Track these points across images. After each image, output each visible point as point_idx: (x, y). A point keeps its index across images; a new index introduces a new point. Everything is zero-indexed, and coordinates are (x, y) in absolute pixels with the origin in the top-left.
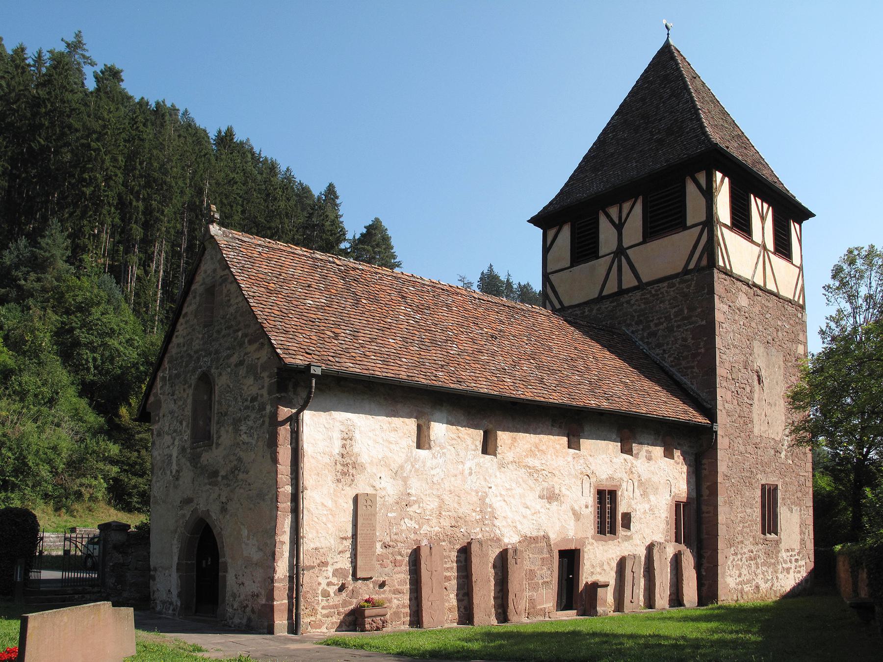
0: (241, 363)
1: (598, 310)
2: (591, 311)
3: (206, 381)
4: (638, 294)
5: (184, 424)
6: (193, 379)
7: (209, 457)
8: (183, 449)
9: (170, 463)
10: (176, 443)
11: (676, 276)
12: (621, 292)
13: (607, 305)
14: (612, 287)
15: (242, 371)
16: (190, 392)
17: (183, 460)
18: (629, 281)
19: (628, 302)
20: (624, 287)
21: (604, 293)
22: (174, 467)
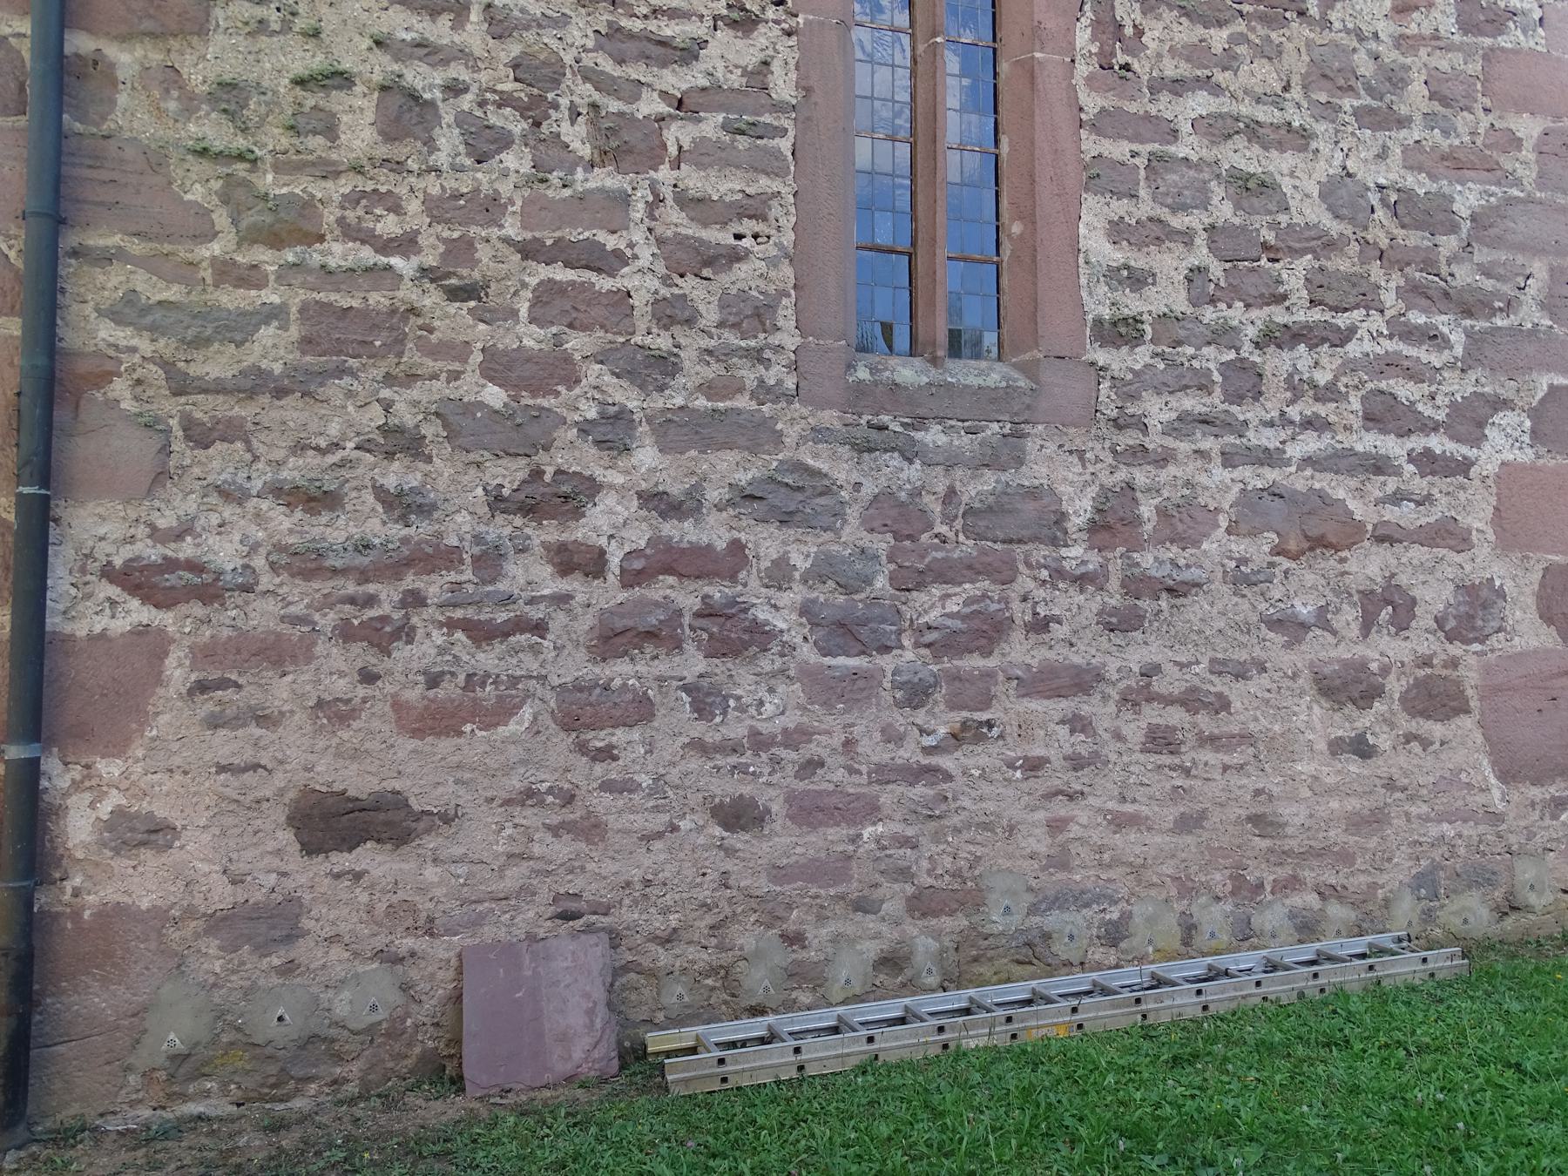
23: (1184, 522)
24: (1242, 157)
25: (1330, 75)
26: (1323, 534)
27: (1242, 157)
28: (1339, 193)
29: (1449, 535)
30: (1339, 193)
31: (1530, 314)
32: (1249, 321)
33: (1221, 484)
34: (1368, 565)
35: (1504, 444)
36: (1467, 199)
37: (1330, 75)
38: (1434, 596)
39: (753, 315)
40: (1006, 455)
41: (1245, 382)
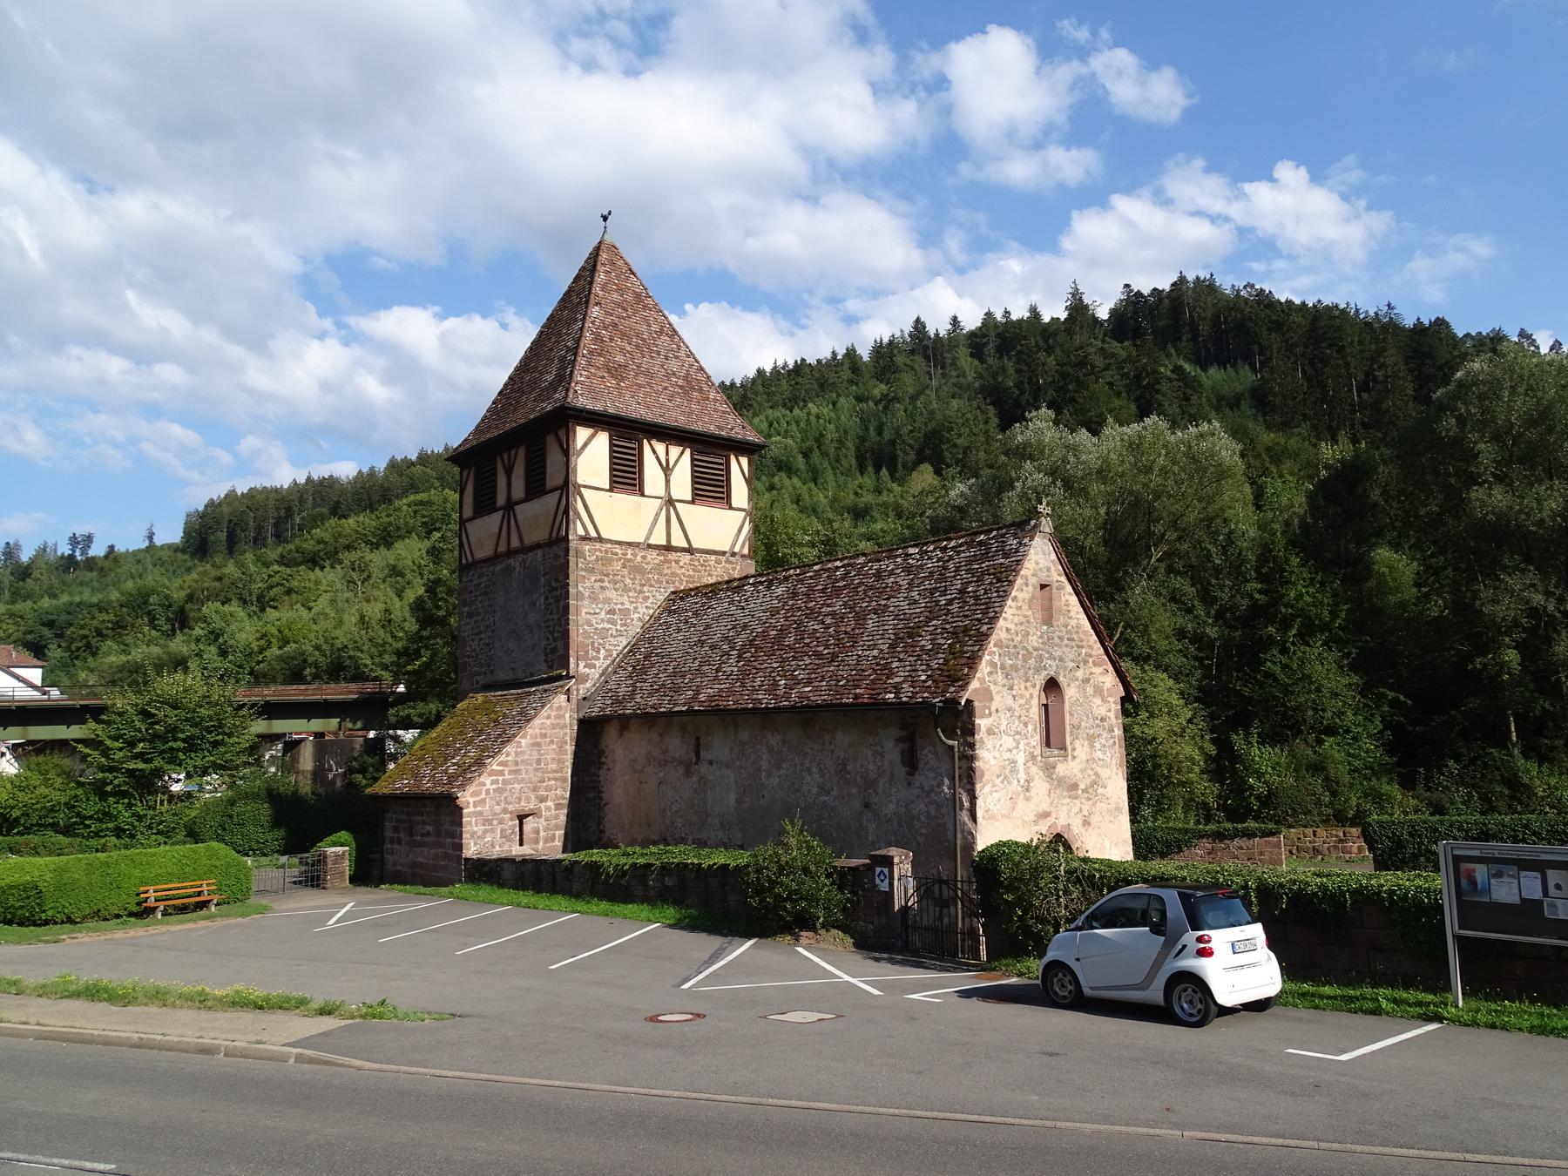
0: (1086, 681)
1: (644, 557)
2: (635, 555)
3: (1052, 686)
4: (688, 557)
5: (1030, 727)
6: (1040, 680)
7: (1062, 769)
8: (1033, 757)
9: (1014, 770)
10: (1021, 746)
11: (724, 553)
12: (668, 548)
13: (653, 556)
14: (659, 538)
15: (1090, 690)
16: (1036, 693)
17: (1034, 769)
18: (678, 540)
19: (677, 562)
20: (674, 543)
21: (651, 541)
22: (1022, 776)
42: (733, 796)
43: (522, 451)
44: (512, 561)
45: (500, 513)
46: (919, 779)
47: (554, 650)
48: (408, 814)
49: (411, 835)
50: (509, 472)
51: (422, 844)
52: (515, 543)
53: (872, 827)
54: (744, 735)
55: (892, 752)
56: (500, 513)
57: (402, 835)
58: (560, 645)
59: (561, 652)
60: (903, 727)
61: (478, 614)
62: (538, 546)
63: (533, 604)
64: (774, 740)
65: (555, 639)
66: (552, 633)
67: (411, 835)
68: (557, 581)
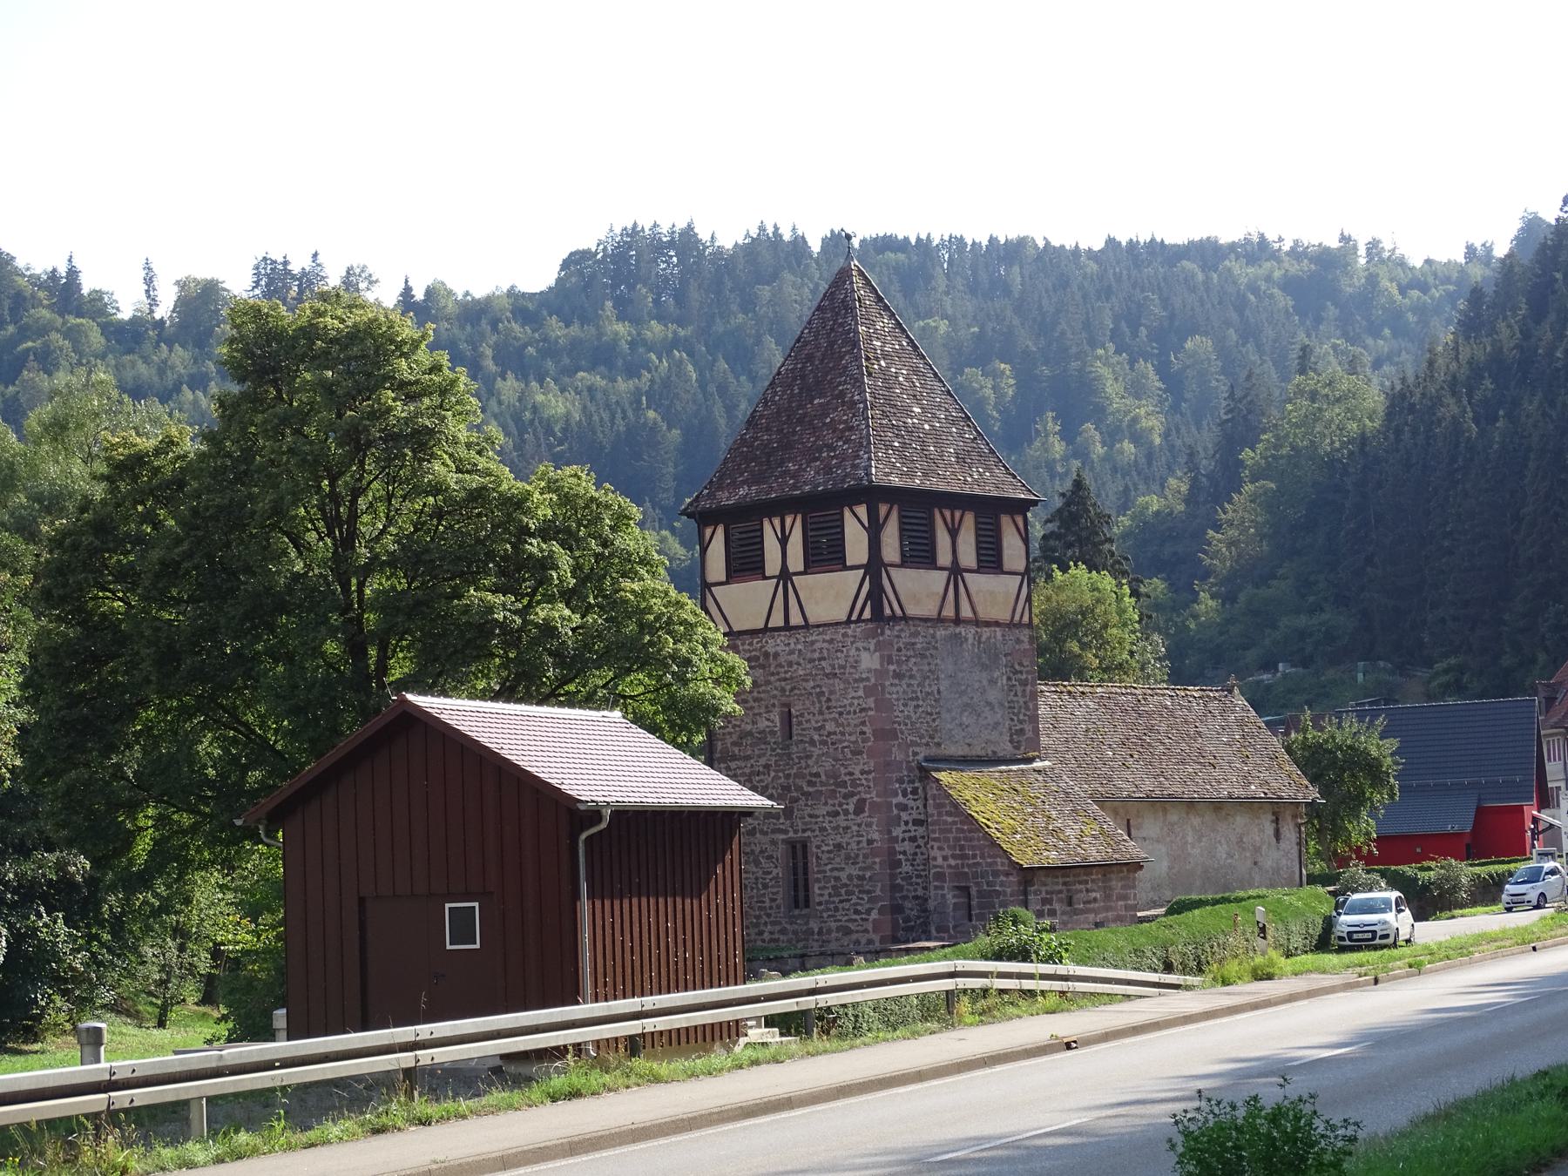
23: (829, 931)
24: (836, 874)
25: (848, 857)
26: (847, 932)
27: (836, 874)
28: (850, 877)
29: (866, 931)
30: (850, 877)
31: (878, 892)
32: (836, 899)
33: (833, 925)
34: (854, 936)
35: (874, 915)
36: (868, 874)
37: (848, 857)
38: (863, 941)
39: (778, 907)
40: (807, 923)
41: (836, 909)
42: (1165, 864)
43: (969, 519)
44: (961, 630)
45: (946, 573)
46: (1282, 845)
47: (1022, 731)
48: (1065, 884)
49: (1070, 904)
50: (954, 533)
51: (1082, 912)
52: (966, 612)
53: (1257, 878)
54: (1173, 817)
55: (1270, 829)
56: (946, 573)
57: (1057, 906)
58: (1028, 727)
59: (1030, 734)
60: (1274, 814)
61: (911, 677)
62: (997, 624)
63: (992, 682)
64: (1196, 821)
65: (1021, 722)
66: (1017, 715)
67: (1070, 904)
68: (1020, 664)
